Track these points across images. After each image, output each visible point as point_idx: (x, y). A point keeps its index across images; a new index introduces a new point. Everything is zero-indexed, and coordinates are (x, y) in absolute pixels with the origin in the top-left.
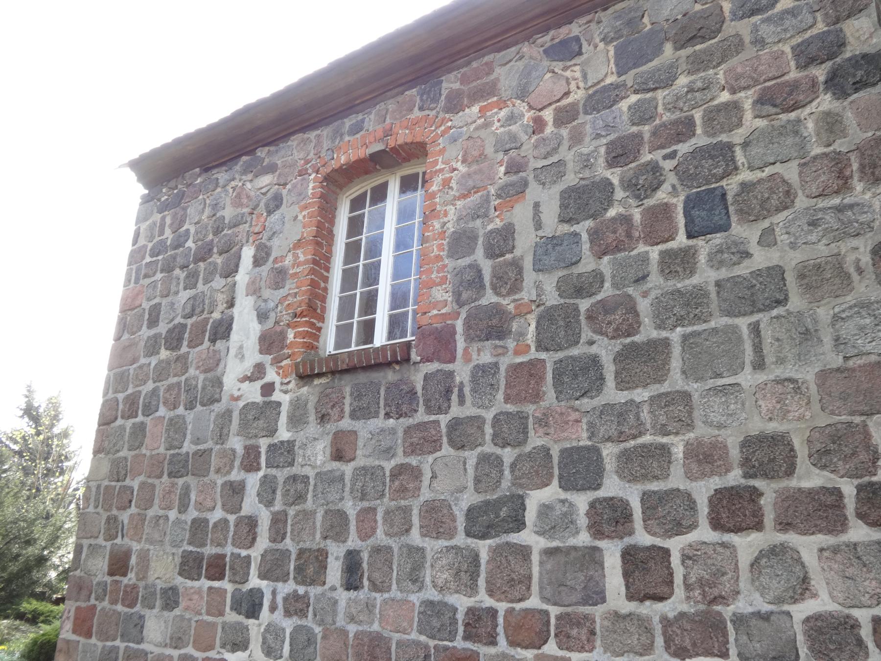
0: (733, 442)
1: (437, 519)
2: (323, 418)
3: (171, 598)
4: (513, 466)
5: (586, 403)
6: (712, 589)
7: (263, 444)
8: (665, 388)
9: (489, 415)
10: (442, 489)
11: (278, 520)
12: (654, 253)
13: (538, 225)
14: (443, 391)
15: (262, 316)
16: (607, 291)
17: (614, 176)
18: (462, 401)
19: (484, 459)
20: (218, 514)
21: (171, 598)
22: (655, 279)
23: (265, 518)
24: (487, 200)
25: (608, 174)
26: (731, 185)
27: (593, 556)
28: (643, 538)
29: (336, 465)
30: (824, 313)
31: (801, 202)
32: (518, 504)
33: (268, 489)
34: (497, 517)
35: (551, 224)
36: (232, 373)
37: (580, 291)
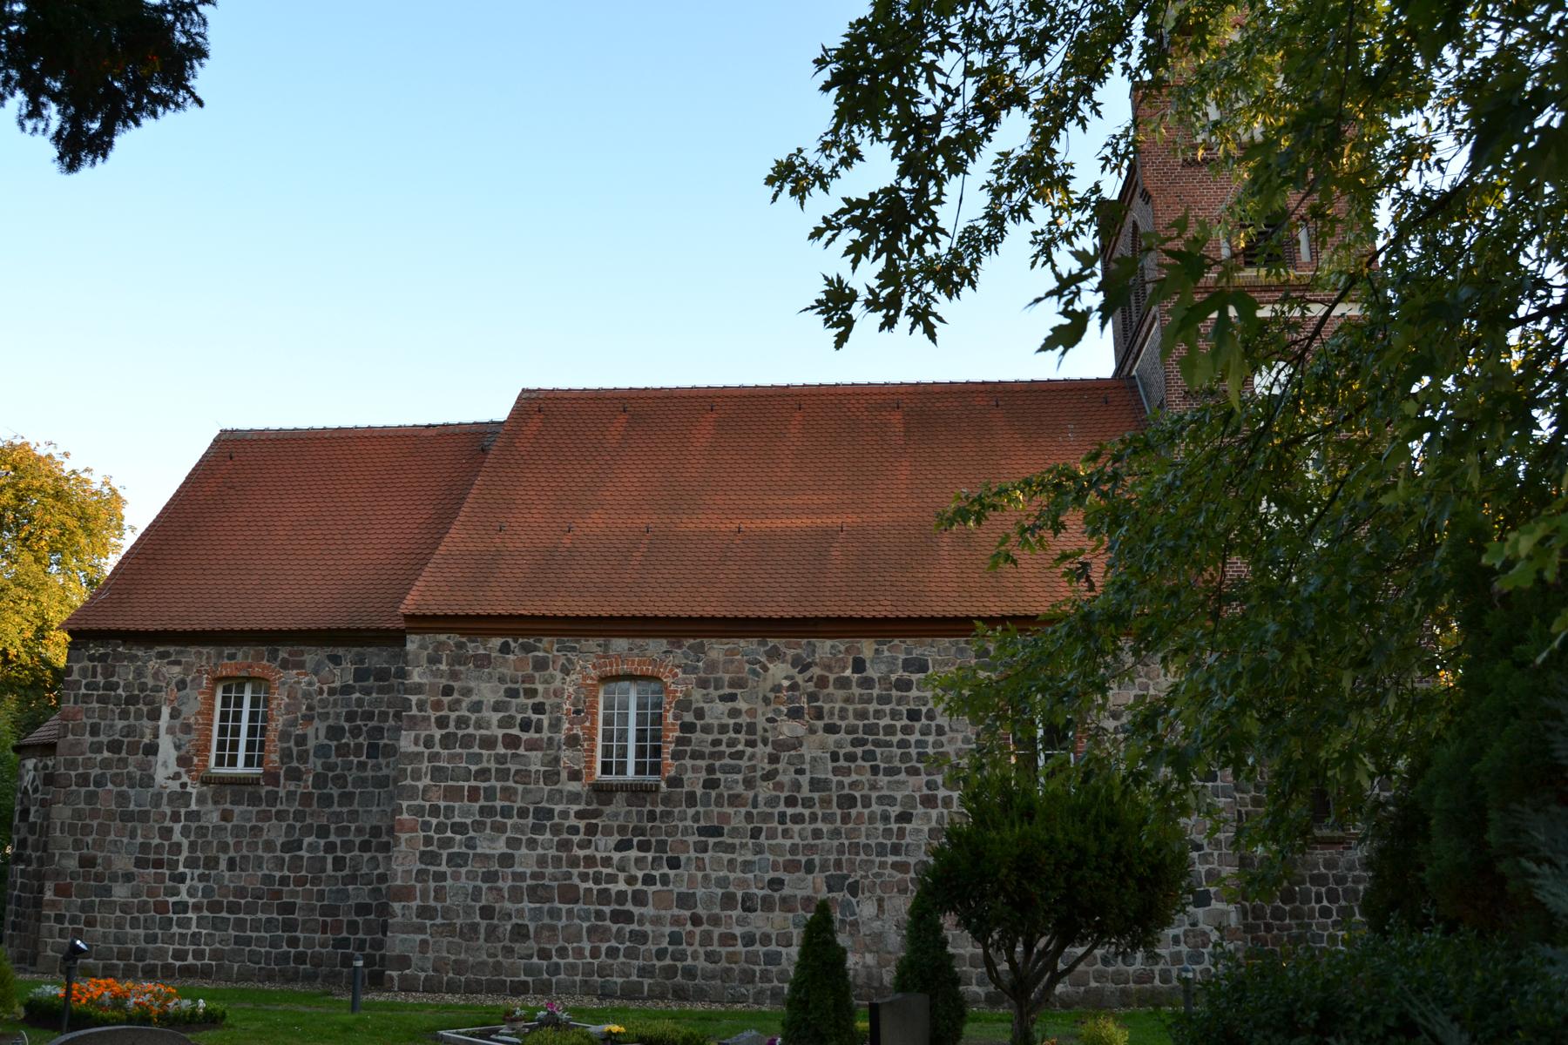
1: (269, 846)
2: (216, 802)
3: (129, 877)
6: (355, 868)
7: (183, 811)
10: (272, 835)
11: (192, 846)
14: (273, 798)
15: (178, 747)
16: (338, 771)
17: (347, 726)
20: (157, 841)
21: (129, 877)
23: (185, 843)
26: (382, 742)
27: (324, 858)
28: (339, 854)
32: (300, 842)
33: (185, 832)
34: (293, 846)
35: (322, 740)
36: (160, 775)
37: (330, 769)
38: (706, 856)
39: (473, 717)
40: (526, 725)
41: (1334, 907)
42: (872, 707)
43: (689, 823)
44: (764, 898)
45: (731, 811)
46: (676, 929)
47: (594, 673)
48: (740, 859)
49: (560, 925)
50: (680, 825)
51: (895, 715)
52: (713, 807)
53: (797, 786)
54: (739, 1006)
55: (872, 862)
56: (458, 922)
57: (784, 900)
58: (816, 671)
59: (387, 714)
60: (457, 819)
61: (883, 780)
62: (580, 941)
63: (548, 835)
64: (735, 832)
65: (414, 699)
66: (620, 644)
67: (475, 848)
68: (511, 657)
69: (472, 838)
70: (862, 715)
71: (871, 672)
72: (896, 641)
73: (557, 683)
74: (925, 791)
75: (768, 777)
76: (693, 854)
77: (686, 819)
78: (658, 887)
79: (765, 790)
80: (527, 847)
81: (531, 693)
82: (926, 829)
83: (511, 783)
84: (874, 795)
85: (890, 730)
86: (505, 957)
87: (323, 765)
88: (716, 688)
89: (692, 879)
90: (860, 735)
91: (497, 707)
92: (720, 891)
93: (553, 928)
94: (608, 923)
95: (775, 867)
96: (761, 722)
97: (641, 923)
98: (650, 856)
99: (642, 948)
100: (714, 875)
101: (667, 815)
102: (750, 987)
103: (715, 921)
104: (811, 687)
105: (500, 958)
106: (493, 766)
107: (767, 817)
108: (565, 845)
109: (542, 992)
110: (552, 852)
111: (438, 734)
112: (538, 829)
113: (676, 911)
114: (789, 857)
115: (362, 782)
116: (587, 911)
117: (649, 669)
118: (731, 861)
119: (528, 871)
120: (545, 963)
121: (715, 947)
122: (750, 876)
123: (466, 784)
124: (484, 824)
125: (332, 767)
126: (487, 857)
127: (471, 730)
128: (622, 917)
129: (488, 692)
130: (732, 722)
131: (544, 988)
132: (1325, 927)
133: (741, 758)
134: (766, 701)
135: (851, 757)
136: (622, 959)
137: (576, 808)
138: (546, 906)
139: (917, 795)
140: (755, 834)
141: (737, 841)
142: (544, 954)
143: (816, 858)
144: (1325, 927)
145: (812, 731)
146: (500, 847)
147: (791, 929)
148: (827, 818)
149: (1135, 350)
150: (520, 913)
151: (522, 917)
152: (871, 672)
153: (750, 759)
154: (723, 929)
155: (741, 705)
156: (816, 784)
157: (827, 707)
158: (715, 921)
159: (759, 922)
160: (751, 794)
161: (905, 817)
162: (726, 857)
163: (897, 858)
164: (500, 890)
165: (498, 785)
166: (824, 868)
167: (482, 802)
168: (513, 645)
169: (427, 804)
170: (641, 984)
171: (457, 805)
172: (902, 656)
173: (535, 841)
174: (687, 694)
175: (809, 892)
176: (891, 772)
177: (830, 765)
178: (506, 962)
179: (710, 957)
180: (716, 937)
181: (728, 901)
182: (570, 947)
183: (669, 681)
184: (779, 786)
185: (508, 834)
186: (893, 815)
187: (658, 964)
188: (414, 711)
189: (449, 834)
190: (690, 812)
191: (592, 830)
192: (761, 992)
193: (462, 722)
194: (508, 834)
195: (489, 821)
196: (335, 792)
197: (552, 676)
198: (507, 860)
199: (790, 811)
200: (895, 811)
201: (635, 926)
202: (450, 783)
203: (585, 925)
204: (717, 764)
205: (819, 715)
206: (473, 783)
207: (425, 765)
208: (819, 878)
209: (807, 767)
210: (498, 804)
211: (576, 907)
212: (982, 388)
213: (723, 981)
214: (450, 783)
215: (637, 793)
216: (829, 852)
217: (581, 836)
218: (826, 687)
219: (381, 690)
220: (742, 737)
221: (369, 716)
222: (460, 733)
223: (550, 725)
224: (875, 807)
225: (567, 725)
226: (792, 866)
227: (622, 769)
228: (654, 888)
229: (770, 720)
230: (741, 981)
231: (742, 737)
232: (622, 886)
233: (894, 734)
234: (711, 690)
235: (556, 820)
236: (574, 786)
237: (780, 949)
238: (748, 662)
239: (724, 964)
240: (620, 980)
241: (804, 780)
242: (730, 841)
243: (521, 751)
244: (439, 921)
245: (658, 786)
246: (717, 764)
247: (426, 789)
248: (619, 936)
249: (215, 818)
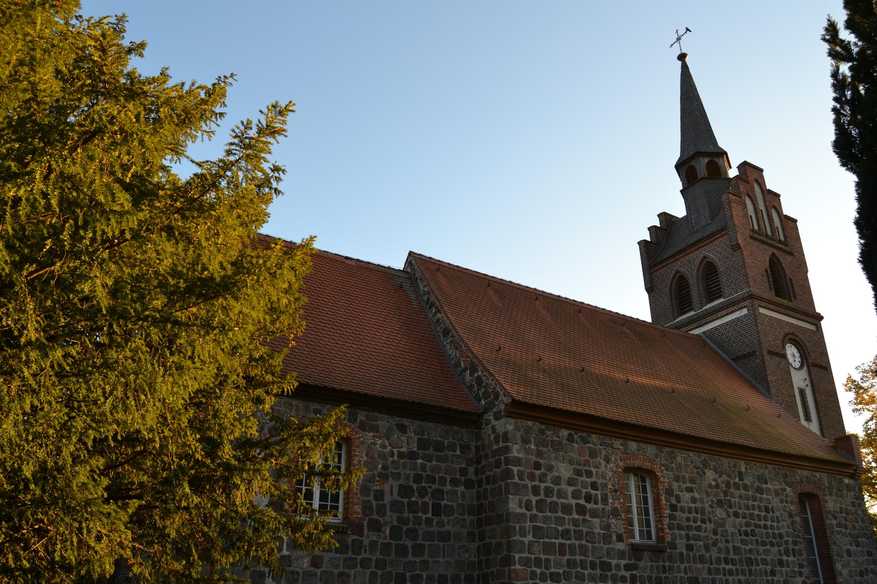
0: (436, 575)
4: (381, 576)
5: (403, 559)
8: (423, 559)
9: (374, 558)
12: (424, 517)
13: (392, 494)
14: (358, 547)
16: (411, 525)
17: (415, 486)
18: (365, 552)
19: (372, 573)
22: (423, 526)
24: (374, 475)
25: (413, 484)
29: (312, 569)
30: (457, 546)
31: (456, 515)
39: (556, 488)
40: (588, 498)
52: (692, 564)
53: (727, 551)
59: (445, 479)
61: (761, 548)
65: (515, 469)
68: (574, 444)
81: (589, 474)
83: (584, 542)
87: (399, 519)
96: (708, 509)
106: (572, 528)
111: (534, 499)
115: (429, 536)
117: (648, 465)
123: (557, 541)
125: (405, 521)
127: (555, 499)
129: (565, 471)
137: (623, 562)
161: (773, 573)
165: (577, 543)
167: (567, 557)
169: (533, 557)
171: (552, 558)
174: (670, 485)
188: (516, 480)
190: (682, 566)
193: (548, 492)
195: (574, 571)
196: (409, 544)
202: (547, 540)
210: (578, 558)
214: (547, 540)
219: (439, 459)
221: (431, 479)
222: (549, 500)
236: (621, 546)
247: (531, 544)
249: (306, 563)
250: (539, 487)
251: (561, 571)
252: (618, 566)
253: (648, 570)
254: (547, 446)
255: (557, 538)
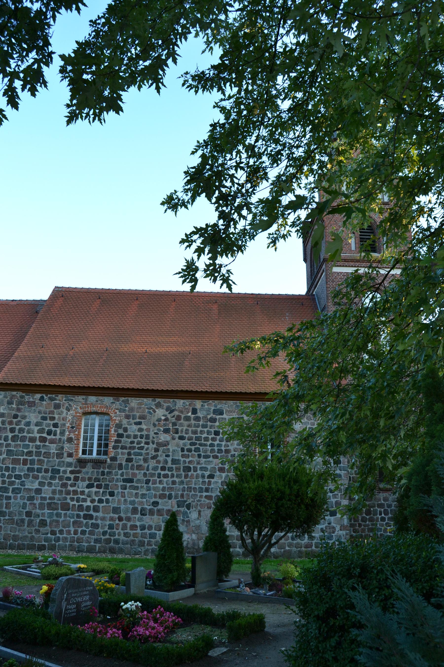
38: (126, 491)
39: (26, 428)
41: (386, 517)
42: (199, 429)
43: (119, 477)
44: (150, 510)
45: (137, 472)
46: (111, 522)
47: (80, 411)
48: (140, 493)
49: (61, 520)
50: (115, 477)
51: (209, 433)
52: (130, 470)
53: (166, 462)
54: (137, 556)
55: (197, 495)
56: (16, 518)
57: (158, 511)
58: (176, 413)
60: (17, 473)
61: (203, 460)
62: (69, 527)
63: (57, 481)
64: (139, 481)
66: (92, 399)
67: (25, 486)
68: (44, 403)
69: (23, 481)
70: (195, 432)
71: (200, 414)
72: (211, 401)
73: (64, 415)
74: (220, 465)
75: (154, 458)
76: (120, 490)
77: (117, 474)
78: (105, 504)
79: (152, 463)
80: (48, 486)
81: (53, 419)
82: (220, 481)
83: (42, 458)
84: (199, 466)
85: (206, 439)
86: (36, 534)
88: (133, 419)
89: (119, 501)
90: (194, 441)
91: (37, 424)
92: (131, 507)
93: (57, 522)
94: (82, 519)
95: (155, 496)
96: (152, 434)
97: (96, 519)
98: (101, 490)
99: (97, 530)
100: (129, 499)
101: (109, 473)
102: (142, 548)
103: (128, 519)
104: (174, 420)
105: (34, 534)
106: (34, 450)
107: (152, 475)
108: (64, 485)
109: (52, 549)
110: (59, 488)
111: (10, 435)
112: (52, 478)
113: (112, 515)
114: (161, 492)
116: (73, 515)
117: (105, 410)
118: (136, 494)
119: (48, 496)
120: (53, 536)
121: (128, 531)
122: (145, 500)
123: (22, 458)
124: (29, 475)
126: (30, 490)
127: (25, 434)
128: (88, 517)
129: (33, 417)
130: (139, 434)
131: (52, 548)
132: (382, 525)
133: (142, 449)
134: (154, 425)
135: (189, 450)
136: (87, 535)
137: (70, 469)
138: (55, 512)
139: (217, 467)
140: (147, 482)
141: (139, 485)
142: (53, 533)
143: (173, 493)
144: (382, 525)
145: (173, 439)
146: (36, 485)
147: (161, 523)
148: (178, 476)
149: (315, 284)
150: (43, 514)
151: (44, 516)
152: (200, 414)
153: (146, 450)
154: (132, 523)
155: (144, 427)
156: (174, 461)
157: (180, 429)
158: (128, 519)
159: (147, 520)
160: (146, 465)
161: (211, 476)
162: (134, 492)
163: (208, 494)
164: (35, 504)
165: (36, 458)
166: (176, 497)
167: (29, 466)
168: (45, 397)
169: (4, 466)
170: (96, 546)
171: (17, 467)
172: (213, 408)
173: (51, 483)
174: (120, 421)
175: (169, 508)
176: (206, 457)
177: (181, 453)
178: (36, 536)
179: (126, 535)
180: (128, 526)
181: (135, 510)
182: (65, 530)
183: (113, 415)
184: (158, 462)
185: (40, 480)
186: (206, 475)
187: (103, 538)
189: (13, 479)
190: (120, 472)
191: (76, 479)
192: (147, 550)
194: (40, 480)
195: (31, 474)
197: (62, 412)
198: (38, 491)
199: (163, 473)
200: (207, 473)
201: (93, 521)
202: (15, 457)
203: (72, 520)
204: (132, 452)
205: (177, 432)
206: (25, 457)
207: (4, 449)
208: (174, 501)
209: (170, 454)
210: (36, 467)
211: (68, 512)
212: (252, 296)
213: (131, 545)
214: (15, 457)
215: (97, 463)
216: (179, 490)
217: (72, 481)
218: (180, 420)
220: (143, 440)
222: (20, 435)
223: (60, 433)
224: (199, 472)
225: (67, 433)
226: (162, 496)
227: (91, 453)
228: (102, 505)
229: (156, 433)
230: (139, 545)
231: (143, 440)
232: (89, 503)
233: (208, 441)
234: (131, 420)
235: (61, 474)
236: (70, 460)
237: (156, 532)
238: (147, 408)
239: (132, 538)
240: (86, 545)
241: (169, 459)
242: (136, 485)
243: (47, 444)
244: (7, 517)
245: (106, 461)
246: (132, 452)
248: (87, 525)
250: (15, 428)
251: (22, 474)
252: (65, 472)
253: (90, 474)
254: (24, 405)
255: (23, 456)
